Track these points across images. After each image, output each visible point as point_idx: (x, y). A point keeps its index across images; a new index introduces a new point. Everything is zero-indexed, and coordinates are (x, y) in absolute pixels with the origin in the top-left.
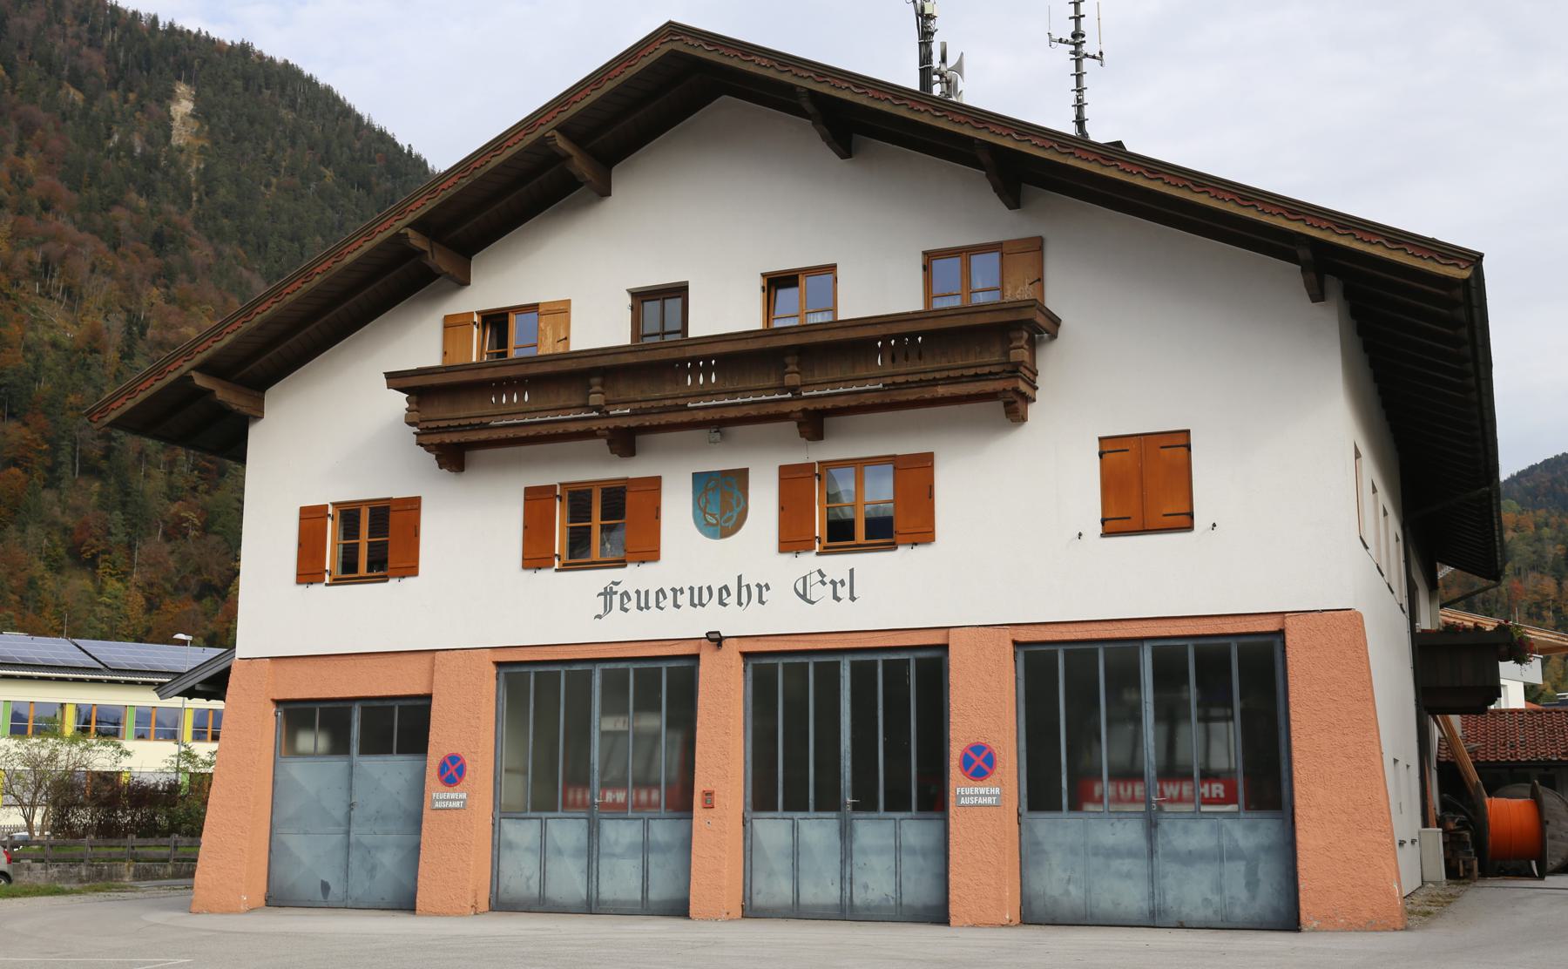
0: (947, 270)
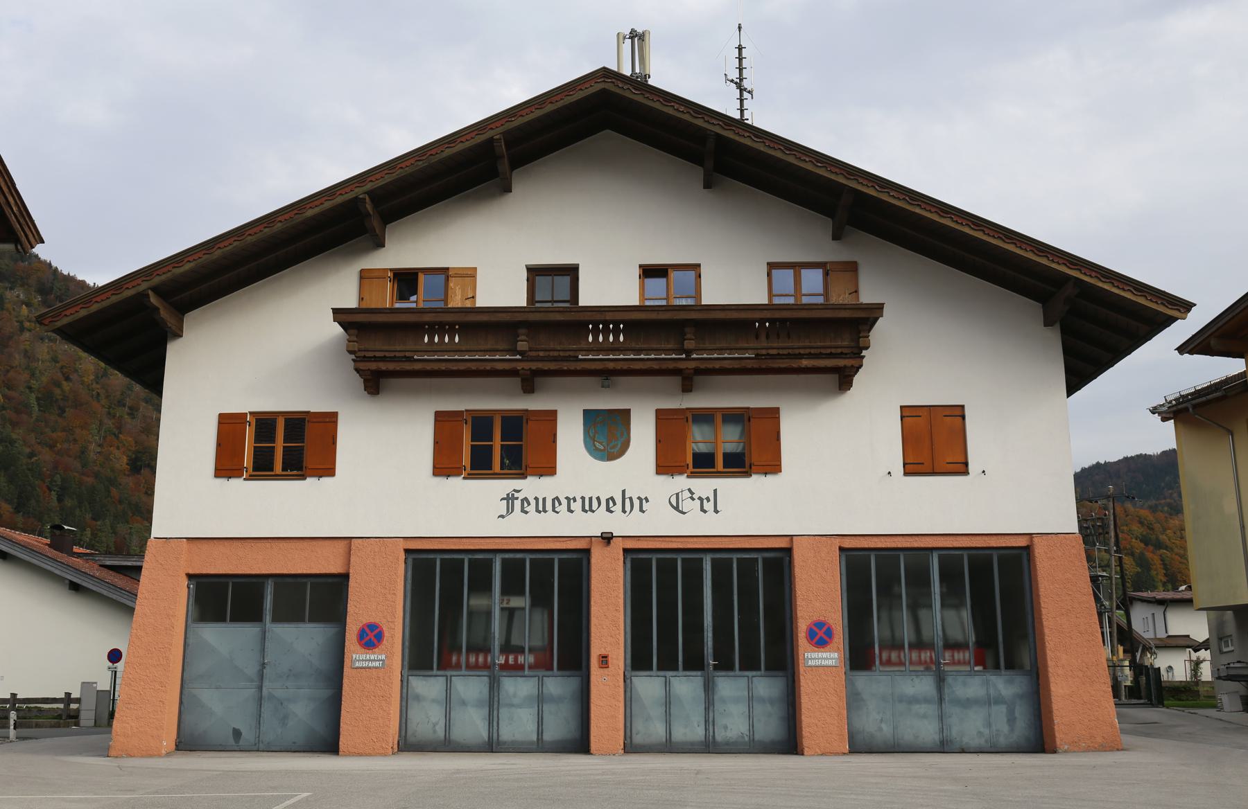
0: (785, 279)
